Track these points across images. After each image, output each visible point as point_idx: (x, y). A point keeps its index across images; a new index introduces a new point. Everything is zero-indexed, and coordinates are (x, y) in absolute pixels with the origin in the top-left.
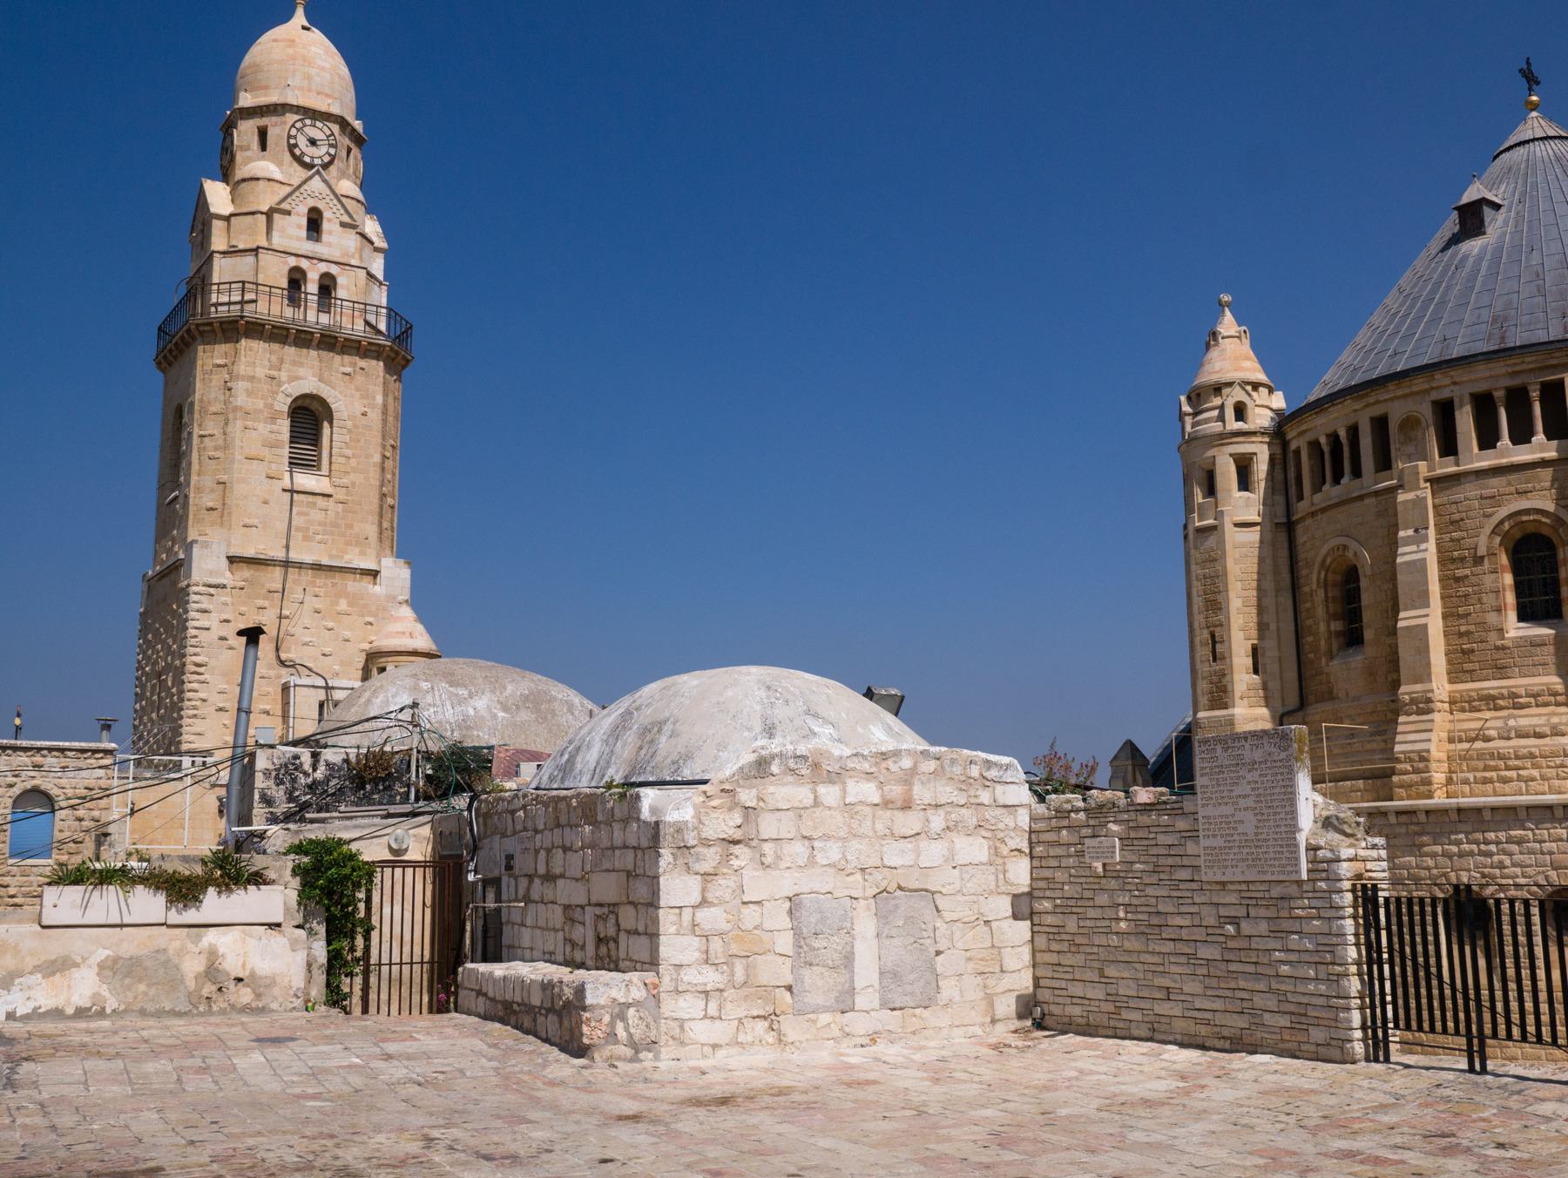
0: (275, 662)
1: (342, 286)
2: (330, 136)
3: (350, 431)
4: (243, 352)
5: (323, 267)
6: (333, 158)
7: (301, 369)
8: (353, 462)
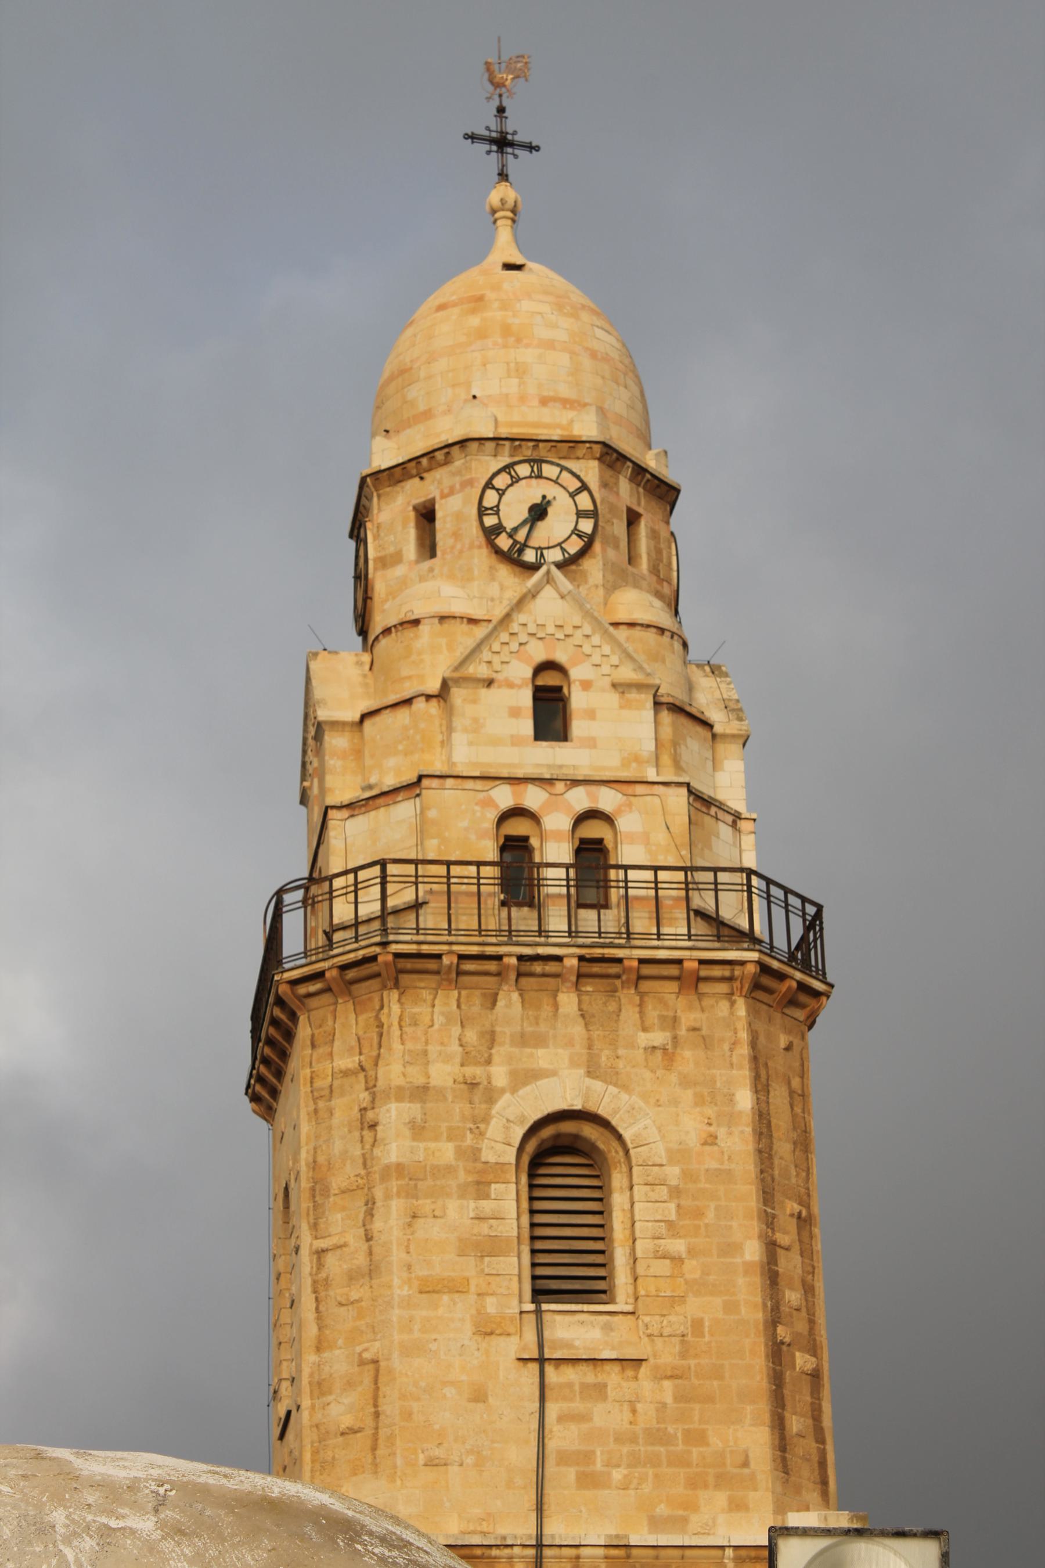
1: (632, 838)
2: (579, 491)
3: (675, 1192)
4: (396, 1032)
5: (580, 800)
7: (541, 1052)
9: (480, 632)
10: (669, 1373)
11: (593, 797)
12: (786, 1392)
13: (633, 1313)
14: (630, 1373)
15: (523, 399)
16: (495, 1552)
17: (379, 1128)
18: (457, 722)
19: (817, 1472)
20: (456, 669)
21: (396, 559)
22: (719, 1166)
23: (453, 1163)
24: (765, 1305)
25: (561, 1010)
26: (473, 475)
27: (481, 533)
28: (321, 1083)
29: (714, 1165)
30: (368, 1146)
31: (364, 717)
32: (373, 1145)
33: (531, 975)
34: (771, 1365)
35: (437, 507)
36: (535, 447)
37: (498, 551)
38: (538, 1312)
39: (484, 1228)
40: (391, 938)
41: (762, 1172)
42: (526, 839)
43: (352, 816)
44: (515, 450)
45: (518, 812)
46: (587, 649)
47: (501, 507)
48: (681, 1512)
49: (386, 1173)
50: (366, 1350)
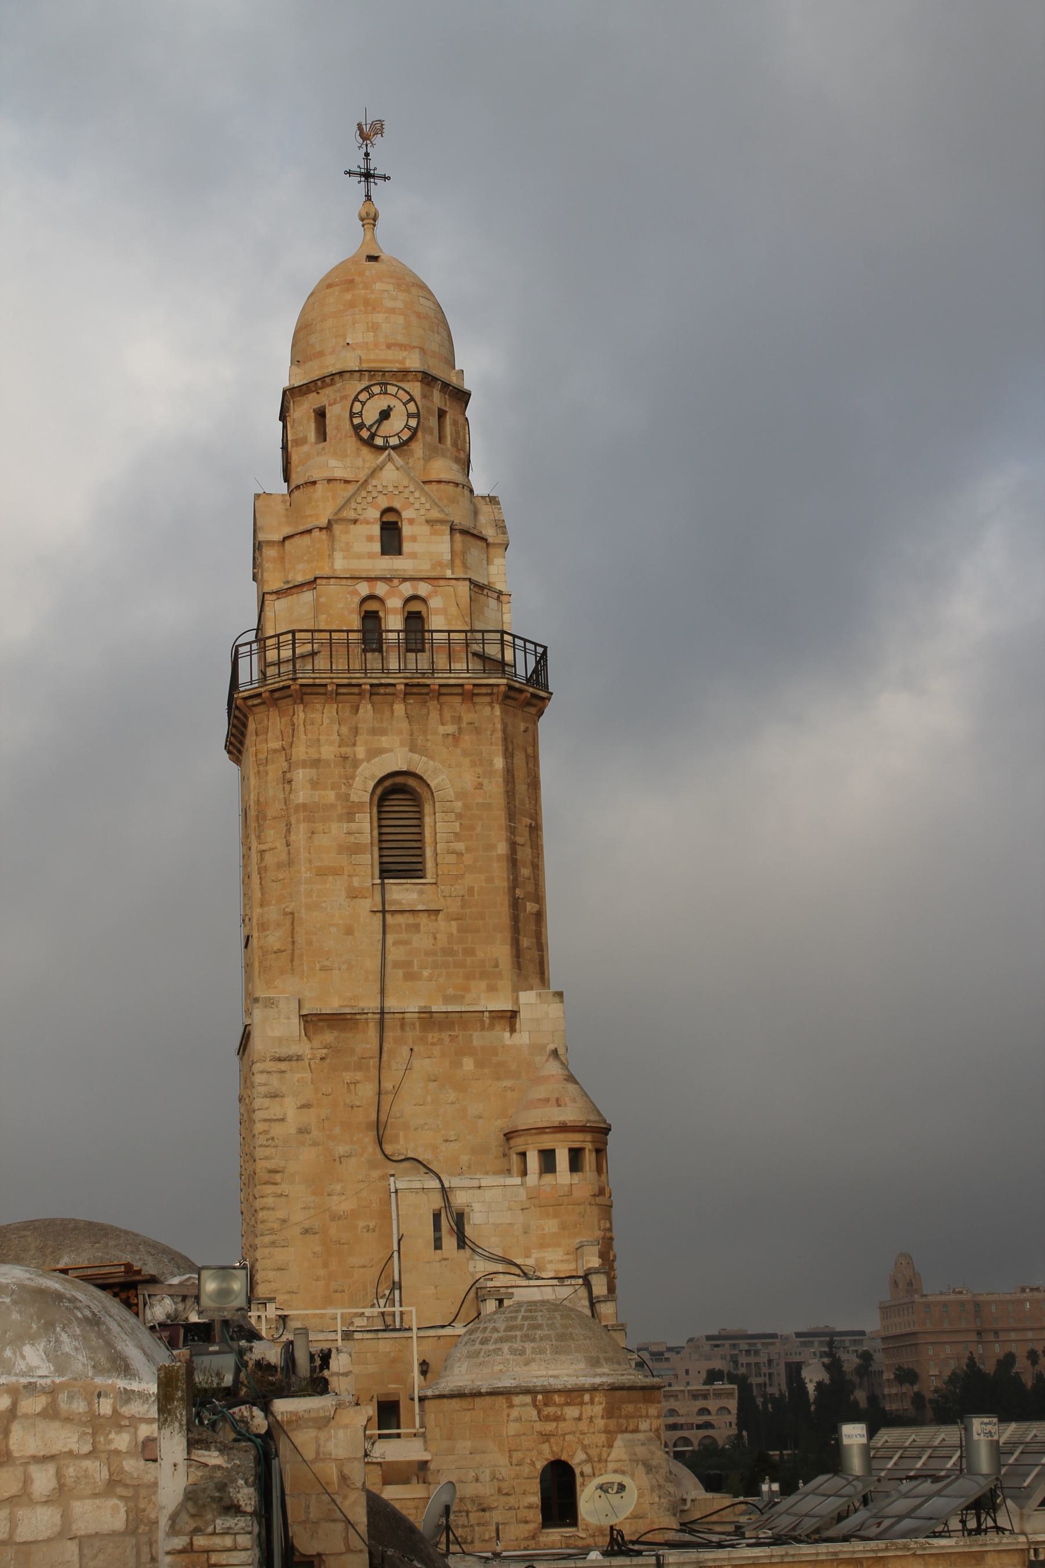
0: (380, 1156)
1: (437, 611)
2: (408, 402)
3: (459, 816)
5: (407, 589)
6: (414, 432)
7: (383, 738)
9: (352, 488)
10: (455, 917)
11: (415, 588)
12: (520, 925)
13: (436, 884)
14: (433, 917)
15: (376, 345)
16: (358, 1017)
17: (293, 783)
18: (337, 546)
19: (538, 968)
20: (336, 514)
21: (303, 441)
22: (484, 801)
23: (335, 802)
24: (509, 878)
25: (395, 714)
26: (347, 393)
27: (352, 428)
28: (260, 756)
29: (480, 800)
30: (287, 793)
31: (285, 539)
32: (290, 793)
33: (378, 694)
34: (512, 911)
35: (327, 411)
36: (383, 375)
37: (361, 439)
38: (383, 884)
39: (352, 839)
40: (299, 675)
41: (508, 803)
42: (377, 612)
43: (278, 598)
44: (371, 378)
45: (371, 597)
46: (412, 500)
47: (363, 413)
48: (461, 993)
49: (297, 808)
50: (287, 907)
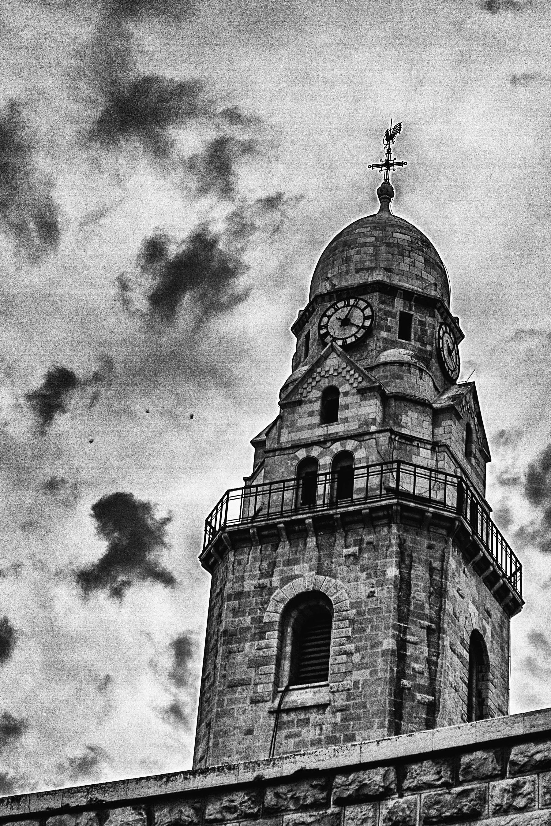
2: (366, 308)
3: (353, 622)
5: (337, 447)
8: (357, 658)
11: (343, 445)
39: (261, 653)
46: (348, 377)
